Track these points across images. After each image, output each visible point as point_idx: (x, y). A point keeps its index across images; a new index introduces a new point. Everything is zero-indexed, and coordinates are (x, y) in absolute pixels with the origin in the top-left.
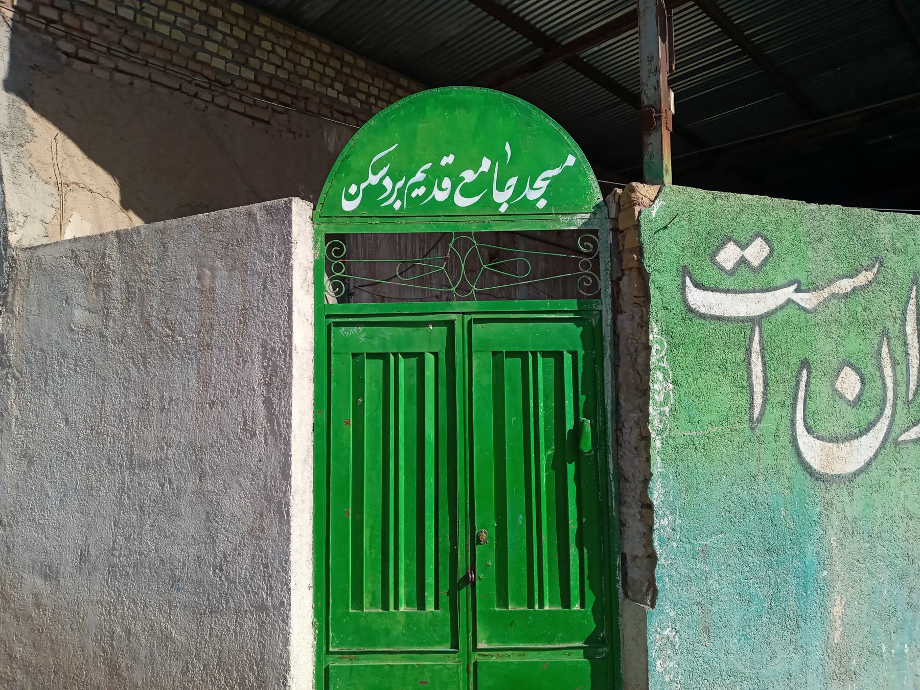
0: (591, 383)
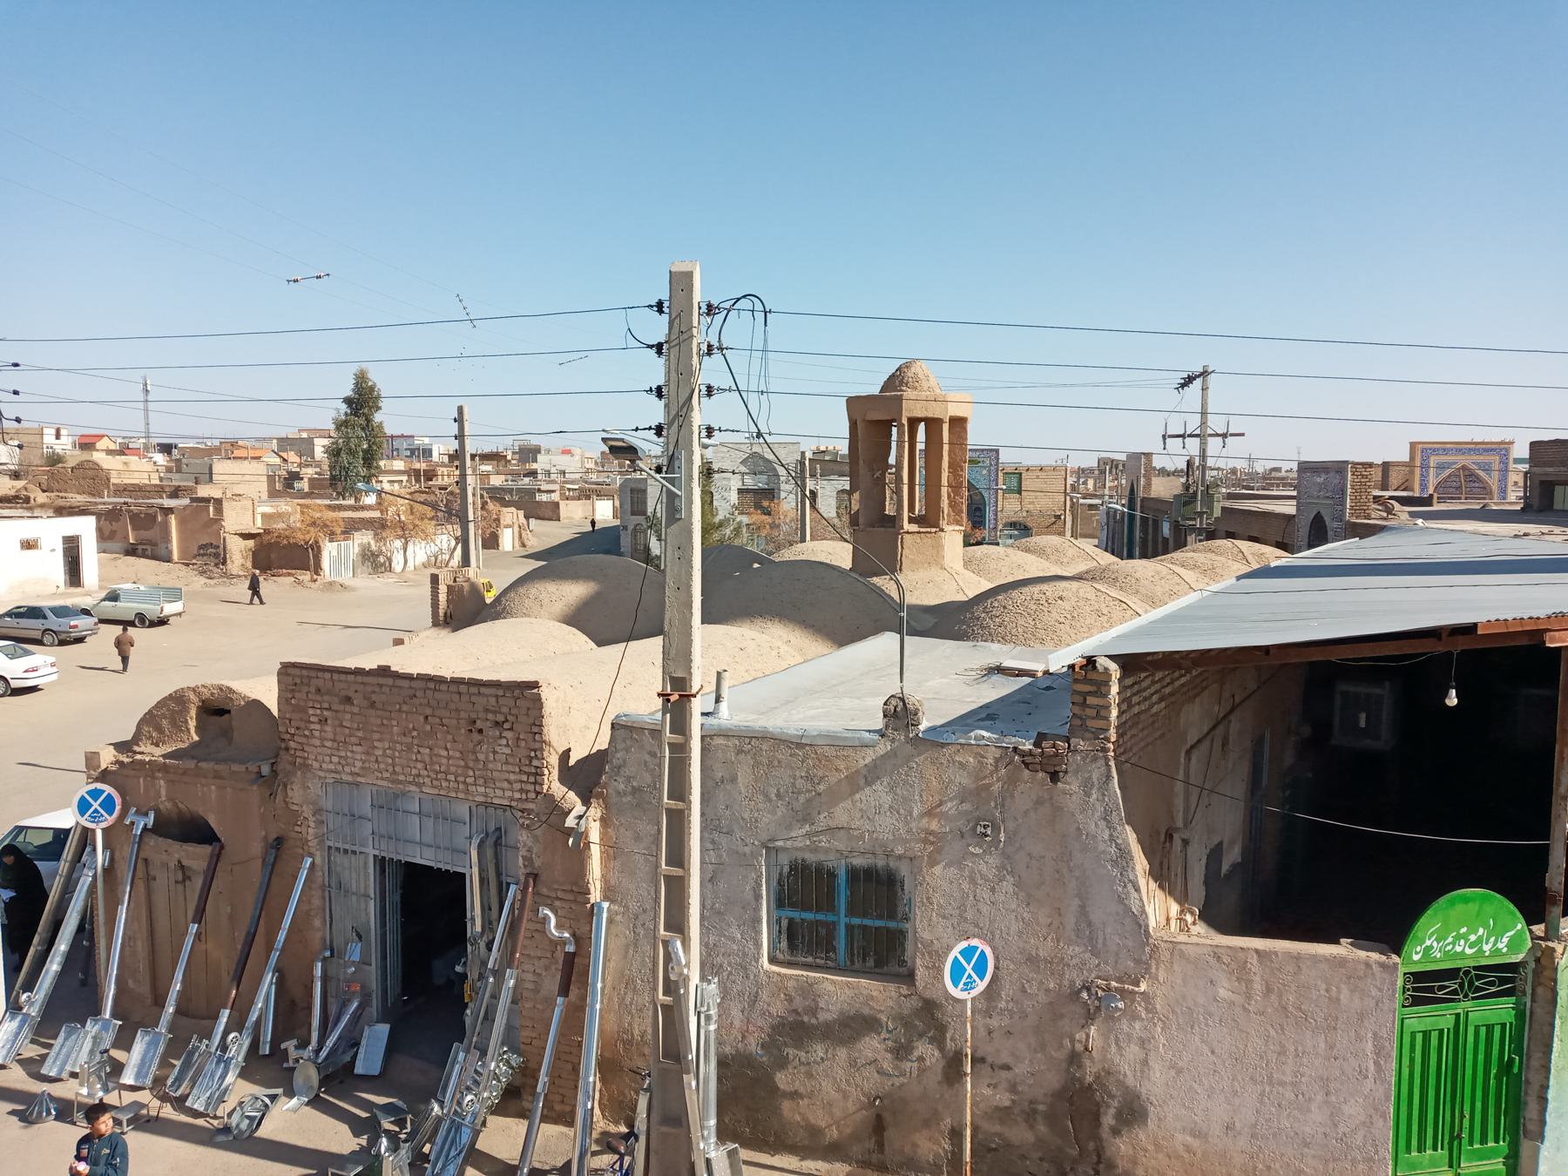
0: (1517, 1039)
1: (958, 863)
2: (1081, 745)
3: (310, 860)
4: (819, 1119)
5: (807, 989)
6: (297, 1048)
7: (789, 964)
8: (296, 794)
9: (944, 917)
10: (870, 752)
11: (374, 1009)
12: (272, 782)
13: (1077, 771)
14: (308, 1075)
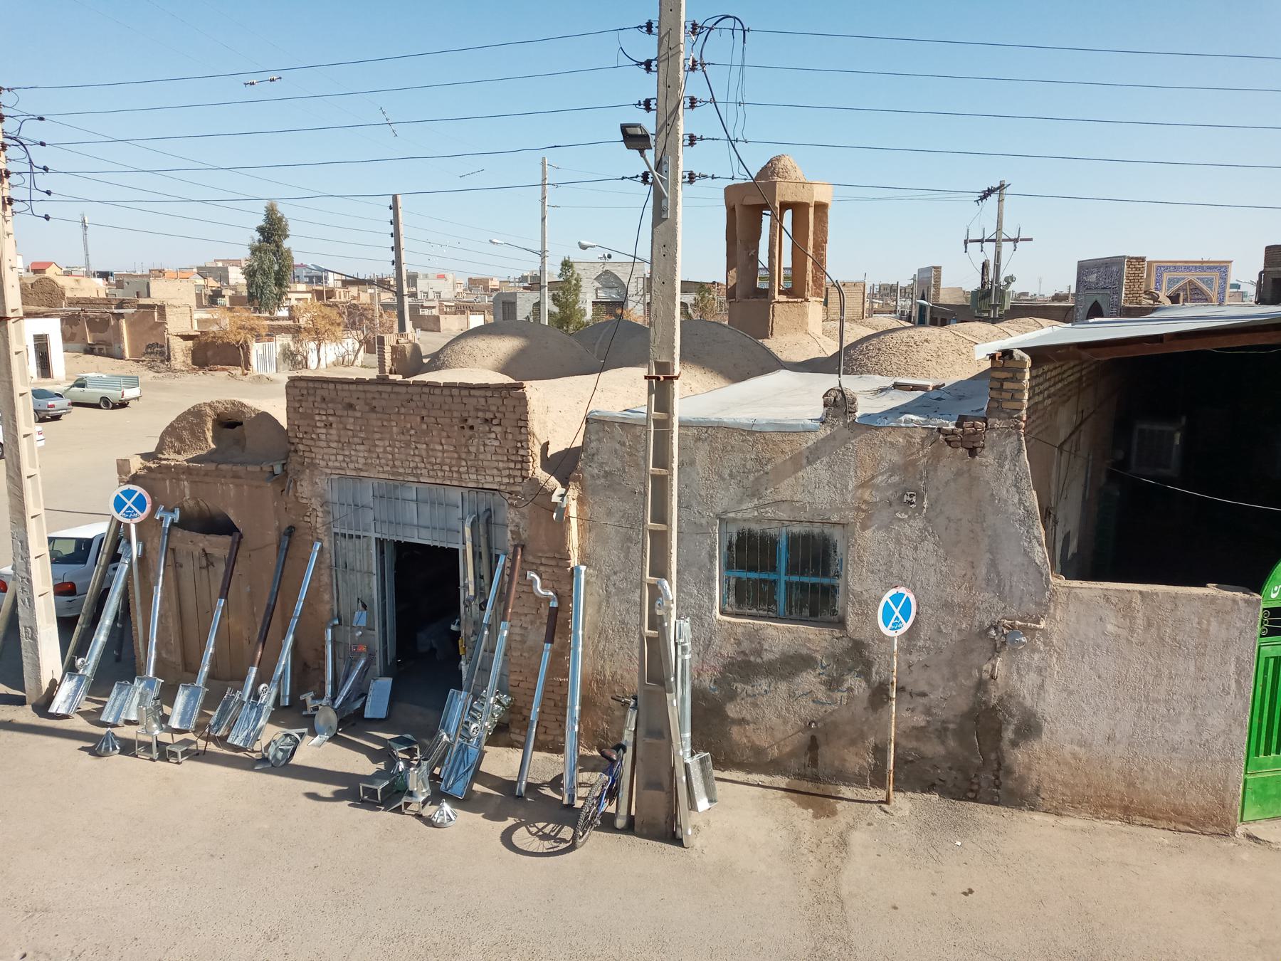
1: (887, 528)
2: (998, 423)
3: (318, 545)
4: (762, 740)
5: (753, 635)
6: (313, 698)
7: (737, 615)
8: (304, 489)
9: (872, 572)
10: (812, 436)
11: (378, 665)
12: (283, 481)
13: (992, 447)
14: (327, 717)
